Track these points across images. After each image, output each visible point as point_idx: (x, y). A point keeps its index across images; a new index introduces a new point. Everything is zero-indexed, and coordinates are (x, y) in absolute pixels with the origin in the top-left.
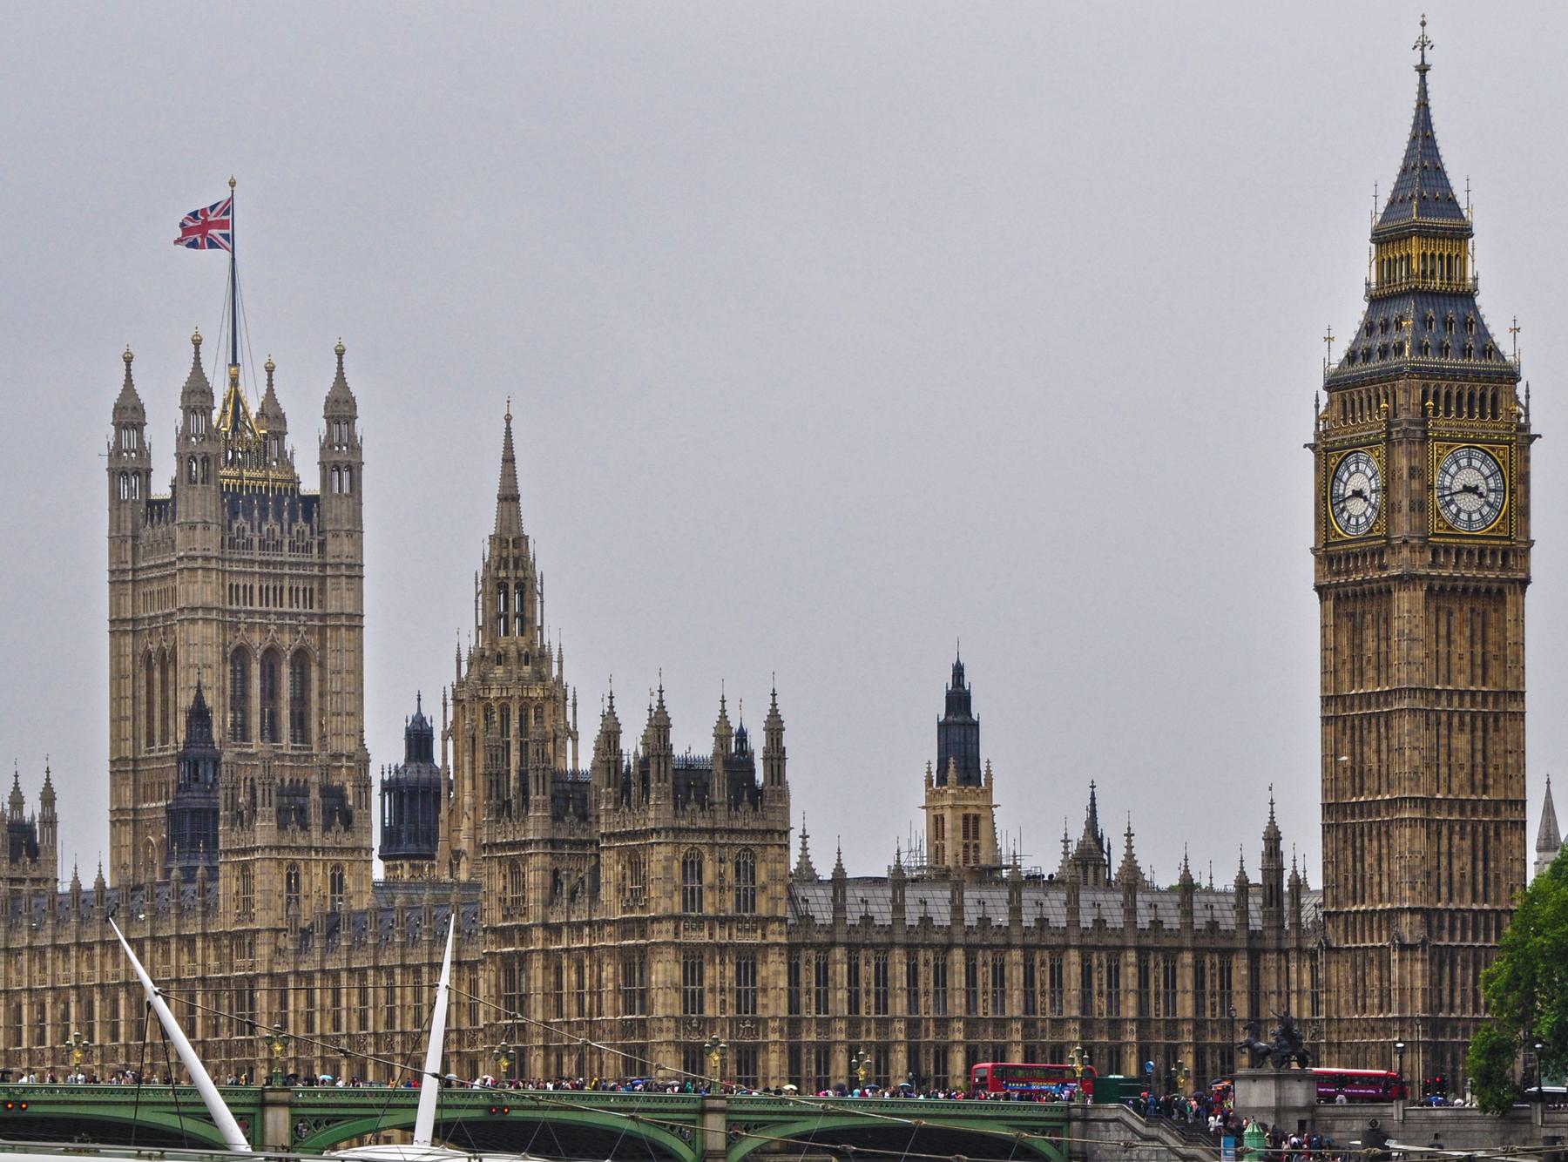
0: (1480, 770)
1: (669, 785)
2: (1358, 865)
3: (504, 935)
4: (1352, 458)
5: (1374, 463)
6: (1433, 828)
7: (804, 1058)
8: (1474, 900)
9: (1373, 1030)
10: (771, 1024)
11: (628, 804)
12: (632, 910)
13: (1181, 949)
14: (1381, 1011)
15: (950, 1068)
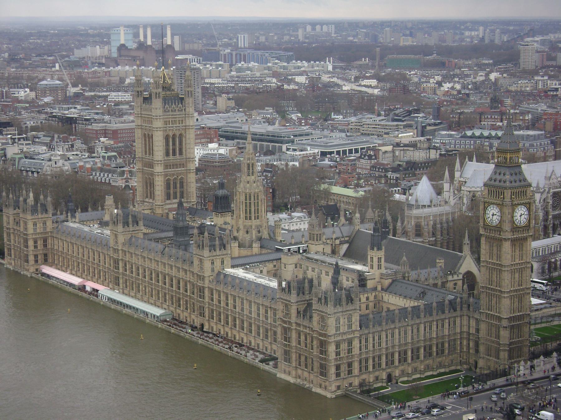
0: (520, 281)
1: (332, 303)
2: (490, 302)
3: (285, 322)
4: (492, 206)
5: (498, 209)
6: (511, 297)
7: (362, 361)
8: (518, 312)
9: (493, 342)
10: (355, 356)
11: (321, 303)
12: (322, 330)
13: (445, 319)
14: (496, 338)
15: (395, 357)
